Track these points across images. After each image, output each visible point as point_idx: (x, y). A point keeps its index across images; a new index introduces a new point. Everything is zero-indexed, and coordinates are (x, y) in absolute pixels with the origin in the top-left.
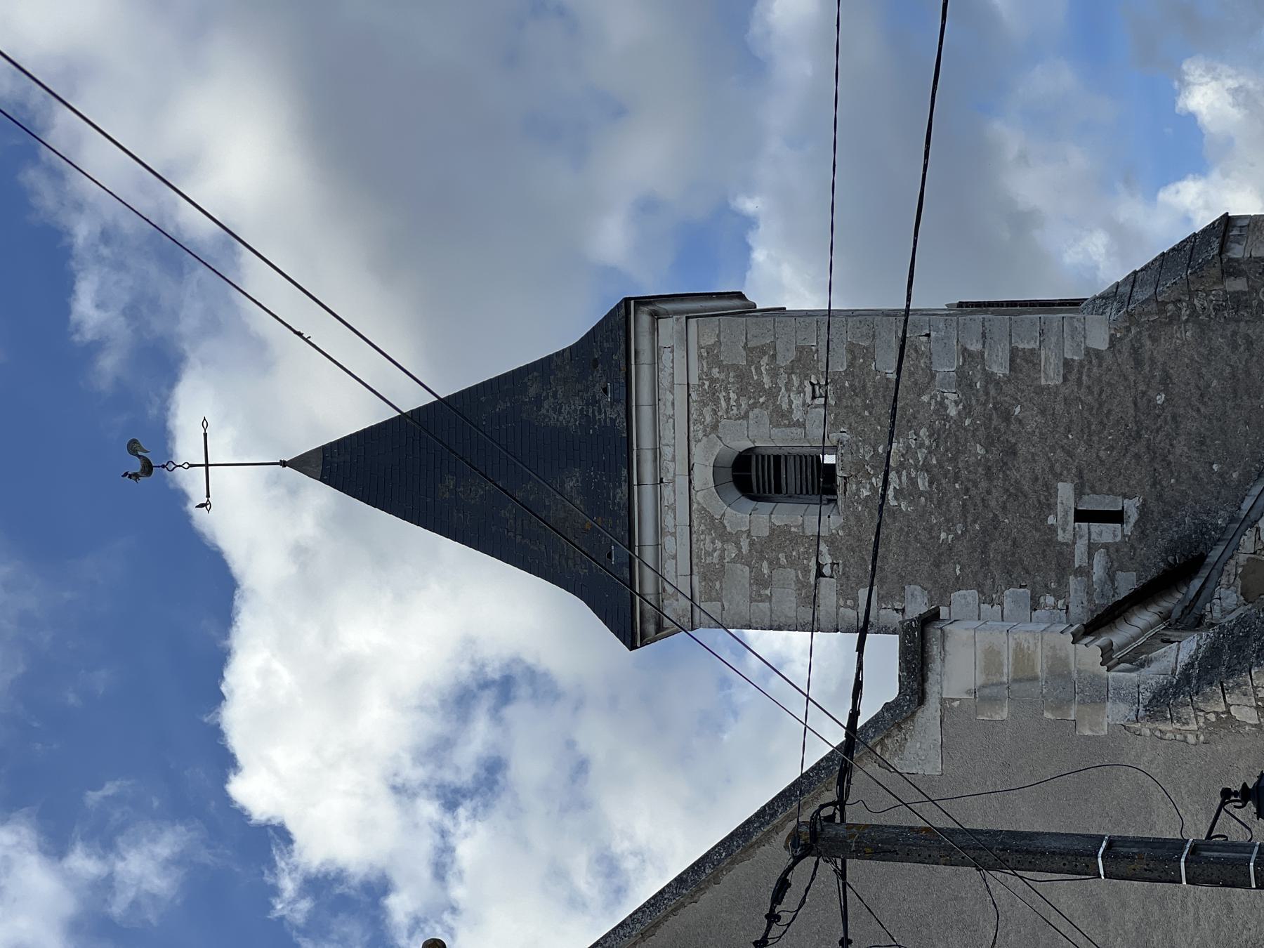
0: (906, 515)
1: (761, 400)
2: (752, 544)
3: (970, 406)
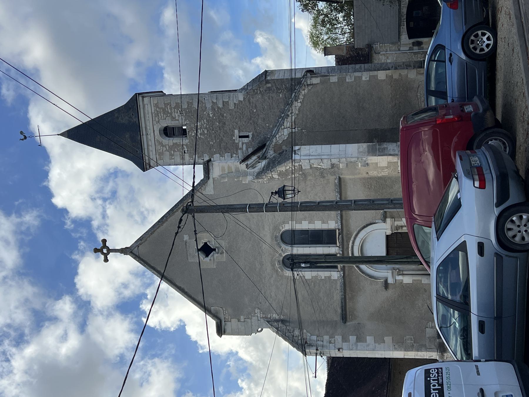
0: (202, 139)
1: (169, 115)
2: (169, 147)
3: (215, 114)
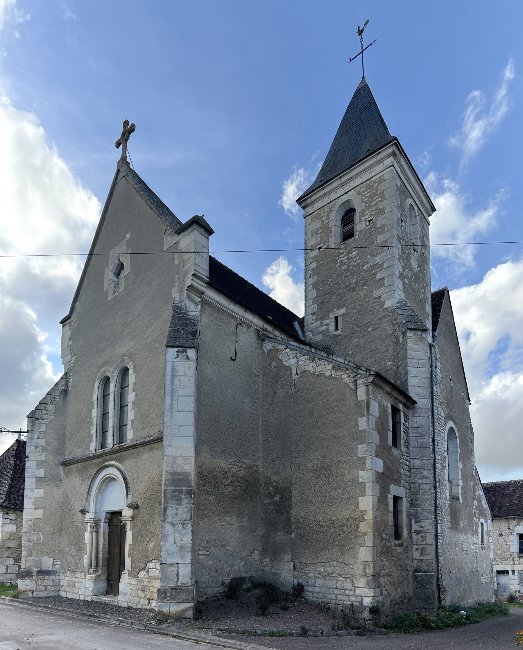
1: (368, 205)
2: (327, 224)
